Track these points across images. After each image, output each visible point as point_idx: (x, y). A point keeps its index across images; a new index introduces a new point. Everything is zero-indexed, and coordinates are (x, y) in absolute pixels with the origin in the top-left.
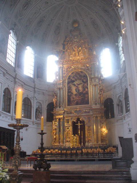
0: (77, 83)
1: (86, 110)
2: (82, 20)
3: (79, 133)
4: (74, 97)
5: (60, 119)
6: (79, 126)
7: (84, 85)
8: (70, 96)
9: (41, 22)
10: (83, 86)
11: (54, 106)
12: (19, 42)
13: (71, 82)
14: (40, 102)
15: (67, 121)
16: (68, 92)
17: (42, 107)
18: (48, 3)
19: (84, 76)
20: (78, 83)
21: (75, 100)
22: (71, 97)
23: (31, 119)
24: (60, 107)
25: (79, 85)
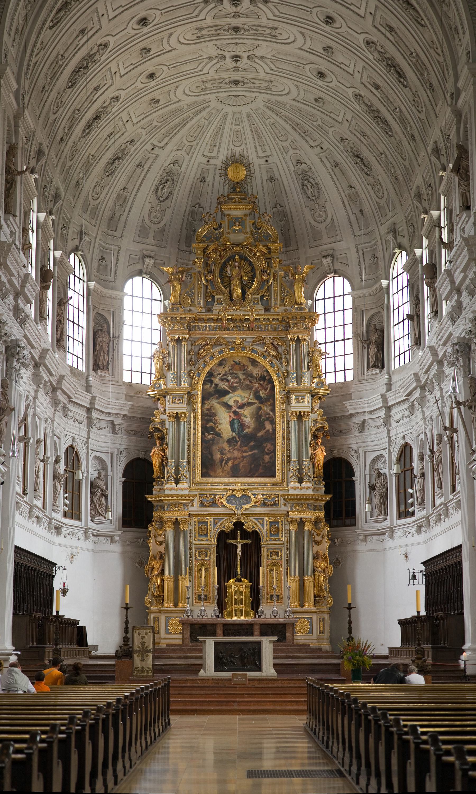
0: (238, 402)
1: (267, 494)
2: (264, 160)
3: (239, 569)
4: (226, 446)
5: (177, 523)
6: (239, 546)
7: (260, 408)
8: (213, 444)
9: (117, 158)
10: (257, 414)
11: (155, 476)
12: (62, 256)
14: (103, 456)
16: (205, 430)
17: (110, 473)
18: (158, 101)
19: (263, 378)
20: (240, 400)
21: (229, 459)
22: (215, 448)
23: (79, 519)
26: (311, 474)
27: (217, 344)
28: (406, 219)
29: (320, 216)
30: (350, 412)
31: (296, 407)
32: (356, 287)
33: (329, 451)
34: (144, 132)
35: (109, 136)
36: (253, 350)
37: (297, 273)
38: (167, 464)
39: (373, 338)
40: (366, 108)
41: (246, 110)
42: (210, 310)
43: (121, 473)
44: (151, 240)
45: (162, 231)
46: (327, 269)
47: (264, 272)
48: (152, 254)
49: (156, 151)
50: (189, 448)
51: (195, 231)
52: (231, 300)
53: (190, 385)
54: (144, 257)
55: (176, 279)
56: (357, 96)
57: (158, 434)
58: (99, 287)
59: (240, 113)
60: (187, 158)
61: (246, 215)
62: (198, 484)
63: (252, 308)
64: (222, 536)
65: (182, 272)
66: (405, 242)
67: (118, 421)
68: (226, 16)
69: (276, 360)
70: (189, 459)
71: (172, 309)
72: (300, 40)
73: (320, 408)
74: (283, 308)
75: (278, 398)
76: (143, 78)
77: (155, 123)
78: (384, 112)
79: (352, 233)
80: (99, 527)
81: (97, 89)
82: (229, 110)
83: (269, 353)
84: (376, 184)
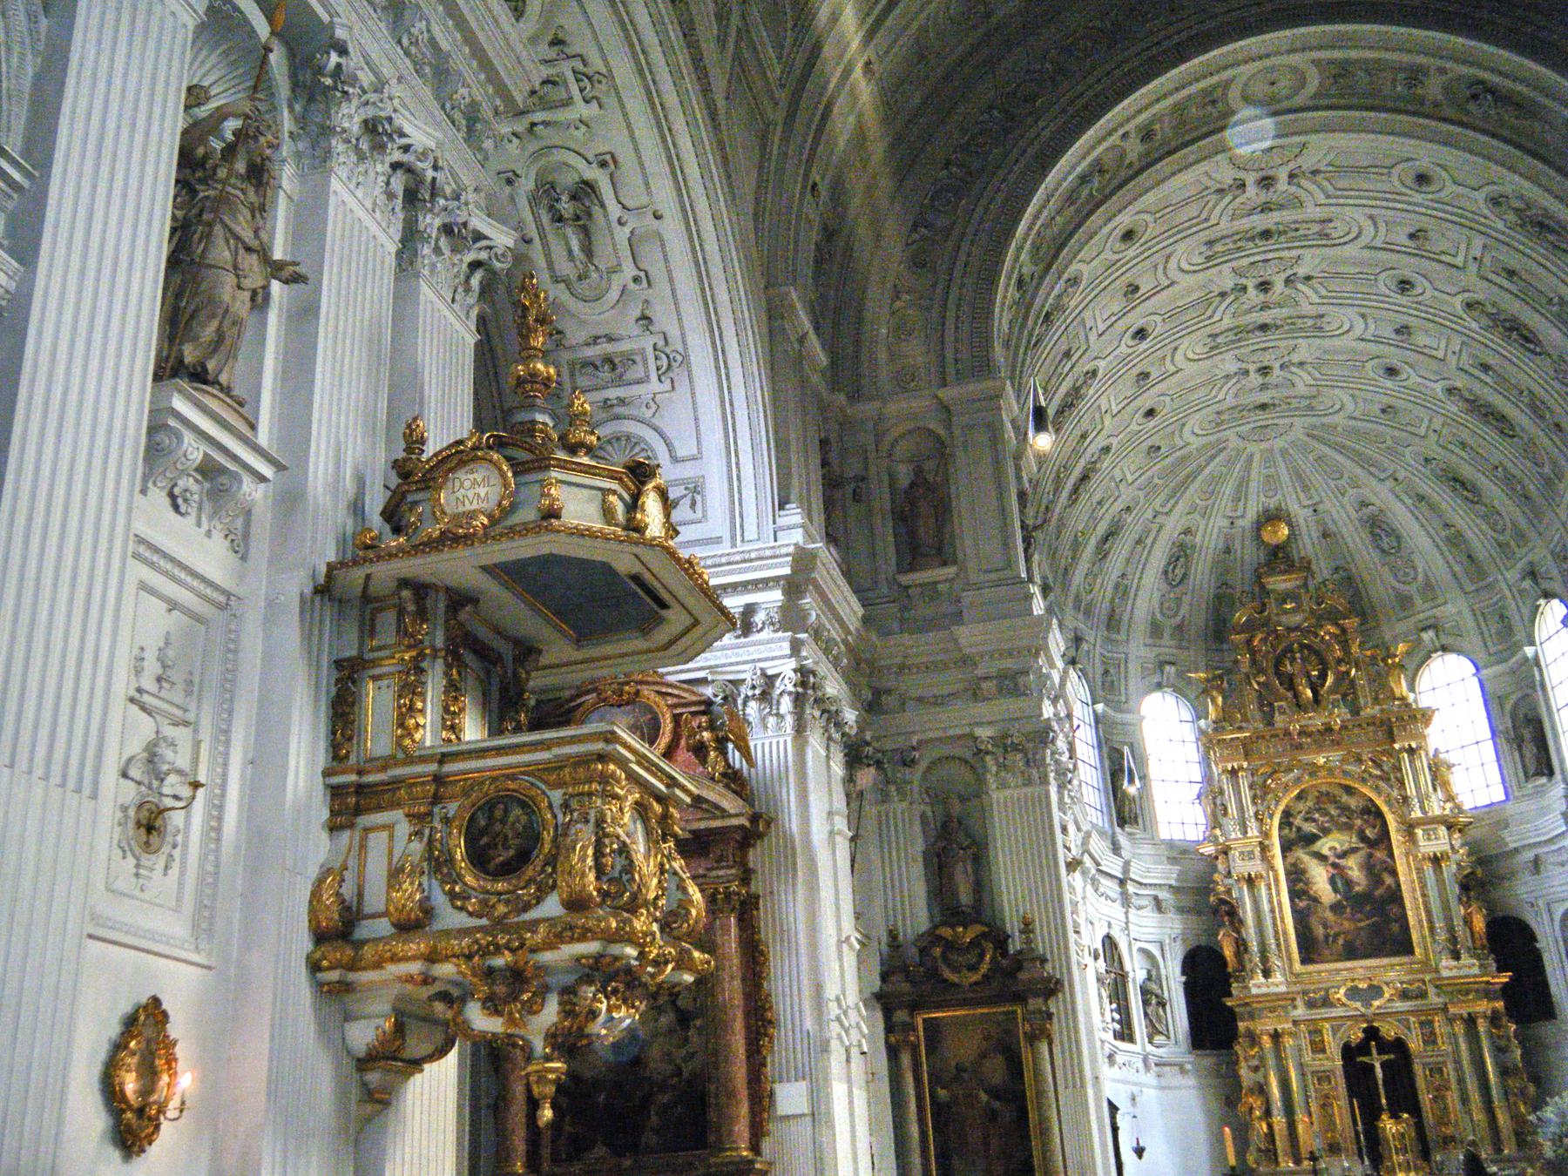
3: (1384, 1101)
4: (1329, 915)
5: (1276, 1036)
7: (1370, 856)
13: (1295, 841)
15: (1312, 1042)
16: (1294, 895)
17: (1163, 972)
18: (1159, 448)
22: (1314, 921)
23: (1131, 1040)
24: (1267, 973)
25: (1344, 855)
26: (1470, 944)
27: (1289, 770)
28: (1552, 553)
29: (1406, 574)
30: (1512, 845)
31: (1427, 847)
32: (1480, 665)
33: (1490, 906)
34: (1141, 494)
35: (1099, 503)
36: (1345, 773)
37: (1389, 656)
38: (1246, 950)
39: (1527, 733)
40: (1466, 405)
41: (1280, 443)
42: (1270, 723)
43: (1178, 970)
44: (1167, 640)
45: (1180, 629)
46: (1431, 647)
47: (1339, 661)
48: (1172, 659)
49: (1160, 519)
50: (1275, 925)
51: (1224, 621)
52: (1299, 706)
53: (1261, 832)
54: (1161, 665)
55: (1213, 687)
56: (1450, 391)
57: (1224, 908)
58: (1110, 712)
59: (1271, 450)
60: (1202, 523)
61: (1299, 587)
62: (1297, 975)
63: (1331, 713)
64: (1349, 1052)
65: (1220, 677)
66: (1556, 586)
67: (1164, 895)
68: (1250, 311)
69: (1381, 784)
70: (1277, 939)
71: (1215, 730)
72: (1359, 325)
73: (1463, 845)
74: (1377, 708)
75: (1396, 837)
76: (1139, 416)
77: (1156, 481)
78: (1498, 401)
79: (1459, 592)
80: (1160, 1051)
81: (1084, 436)
82: (1252, 447)
83: (1370, 774)
84: (1491, 516)
